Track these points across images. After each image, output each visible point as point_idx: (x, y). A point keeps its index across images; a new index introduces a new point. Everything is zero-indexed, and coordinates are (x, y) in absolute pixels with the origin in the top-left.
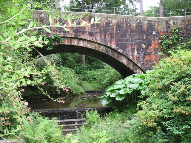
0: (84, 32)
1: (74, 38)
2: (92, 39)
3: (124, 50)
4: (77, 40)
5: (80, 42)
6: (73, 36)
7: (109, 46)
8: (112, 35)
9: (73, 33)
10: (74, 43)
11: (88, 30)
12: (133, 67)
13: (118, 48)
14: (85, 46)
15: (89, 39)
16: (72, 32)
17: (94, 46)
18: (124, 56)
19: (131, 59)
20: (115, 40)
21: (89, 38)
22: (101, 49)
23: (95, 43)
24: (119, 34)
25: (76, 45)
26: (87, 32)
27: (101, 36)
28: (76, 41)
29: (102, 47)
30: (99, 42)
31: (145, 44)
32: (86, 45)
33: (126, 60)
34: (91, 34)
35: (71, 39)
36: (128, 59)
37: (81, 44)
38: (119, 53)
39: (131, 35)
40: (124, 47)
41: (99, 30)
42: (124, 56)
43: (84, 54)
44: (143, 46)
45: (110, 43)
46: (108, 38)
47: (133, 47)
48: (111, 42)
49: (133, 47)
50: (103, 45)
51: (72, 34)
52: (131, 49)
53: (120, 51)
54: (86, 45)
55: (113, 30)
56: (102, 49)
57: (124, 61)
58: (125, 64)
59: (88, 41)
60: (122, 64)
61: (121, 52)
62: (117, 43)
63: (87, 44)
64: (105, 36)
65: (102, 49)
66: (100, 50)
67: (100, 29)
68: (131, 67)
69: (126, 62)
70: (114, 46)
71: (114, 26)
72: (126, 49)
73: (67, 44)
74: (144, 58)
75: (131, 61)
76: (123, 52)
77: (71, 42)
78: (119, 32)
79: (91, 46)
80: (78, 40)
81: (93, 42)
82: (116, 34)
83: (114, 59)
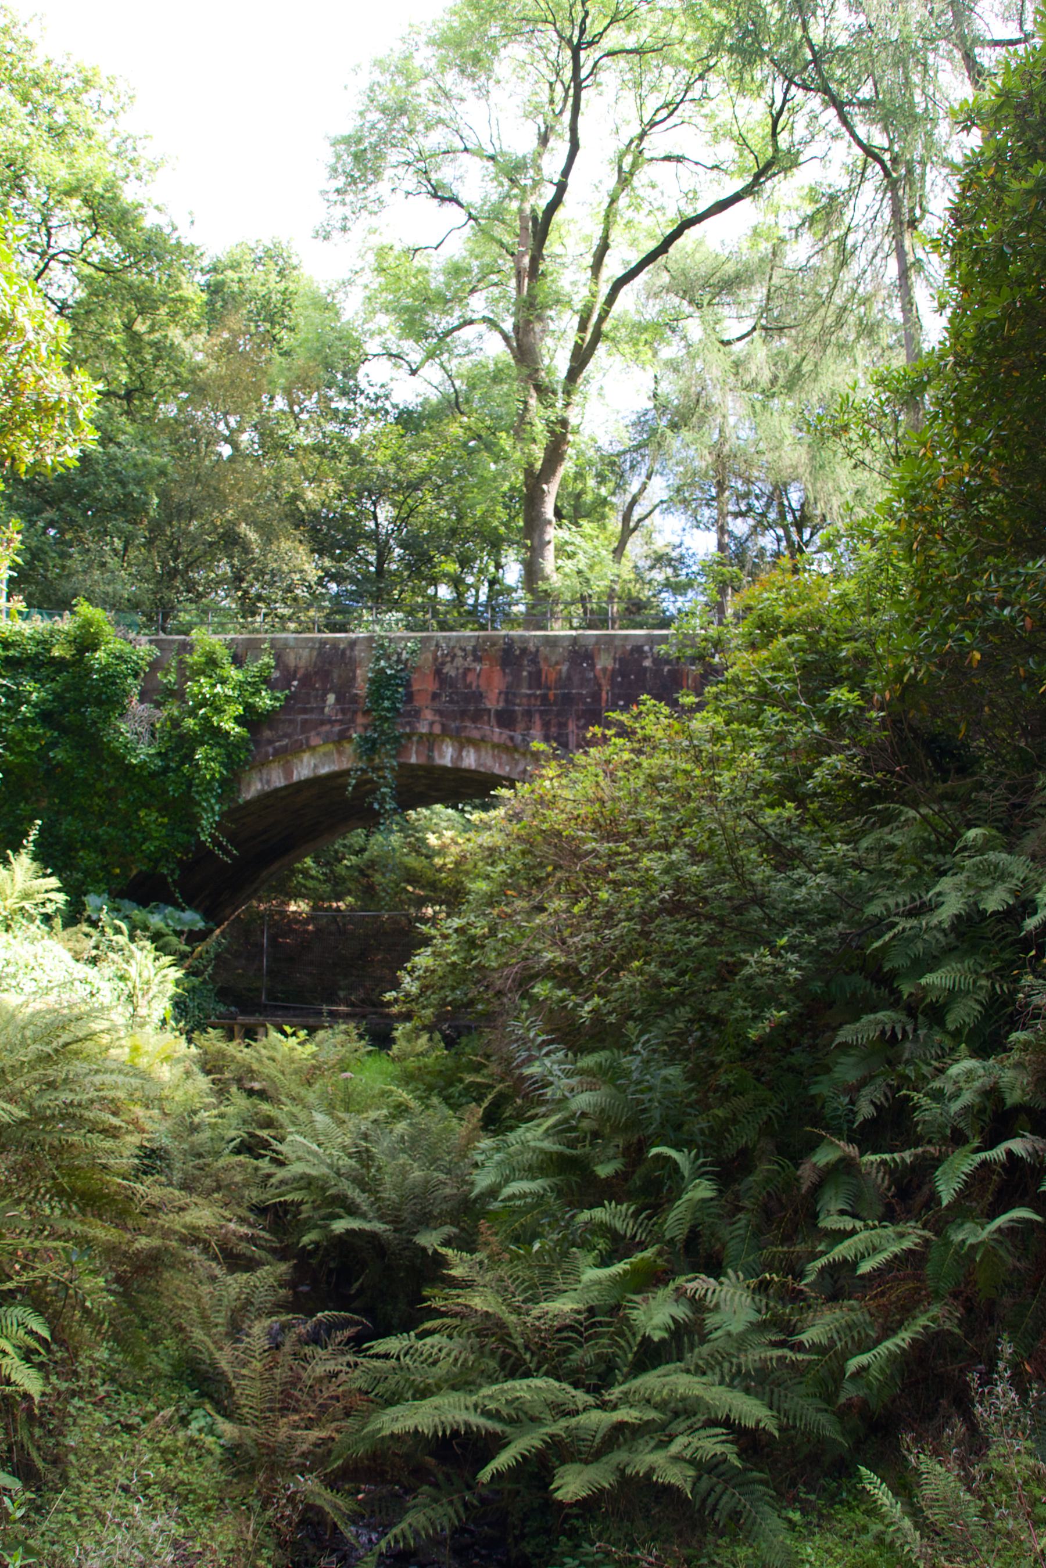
10: (442, 756)
32: (489, 762)
54: (489, 762)
64: (563, 725)
67: (544, 698)
71: (603, 682)
73: (413, 760)
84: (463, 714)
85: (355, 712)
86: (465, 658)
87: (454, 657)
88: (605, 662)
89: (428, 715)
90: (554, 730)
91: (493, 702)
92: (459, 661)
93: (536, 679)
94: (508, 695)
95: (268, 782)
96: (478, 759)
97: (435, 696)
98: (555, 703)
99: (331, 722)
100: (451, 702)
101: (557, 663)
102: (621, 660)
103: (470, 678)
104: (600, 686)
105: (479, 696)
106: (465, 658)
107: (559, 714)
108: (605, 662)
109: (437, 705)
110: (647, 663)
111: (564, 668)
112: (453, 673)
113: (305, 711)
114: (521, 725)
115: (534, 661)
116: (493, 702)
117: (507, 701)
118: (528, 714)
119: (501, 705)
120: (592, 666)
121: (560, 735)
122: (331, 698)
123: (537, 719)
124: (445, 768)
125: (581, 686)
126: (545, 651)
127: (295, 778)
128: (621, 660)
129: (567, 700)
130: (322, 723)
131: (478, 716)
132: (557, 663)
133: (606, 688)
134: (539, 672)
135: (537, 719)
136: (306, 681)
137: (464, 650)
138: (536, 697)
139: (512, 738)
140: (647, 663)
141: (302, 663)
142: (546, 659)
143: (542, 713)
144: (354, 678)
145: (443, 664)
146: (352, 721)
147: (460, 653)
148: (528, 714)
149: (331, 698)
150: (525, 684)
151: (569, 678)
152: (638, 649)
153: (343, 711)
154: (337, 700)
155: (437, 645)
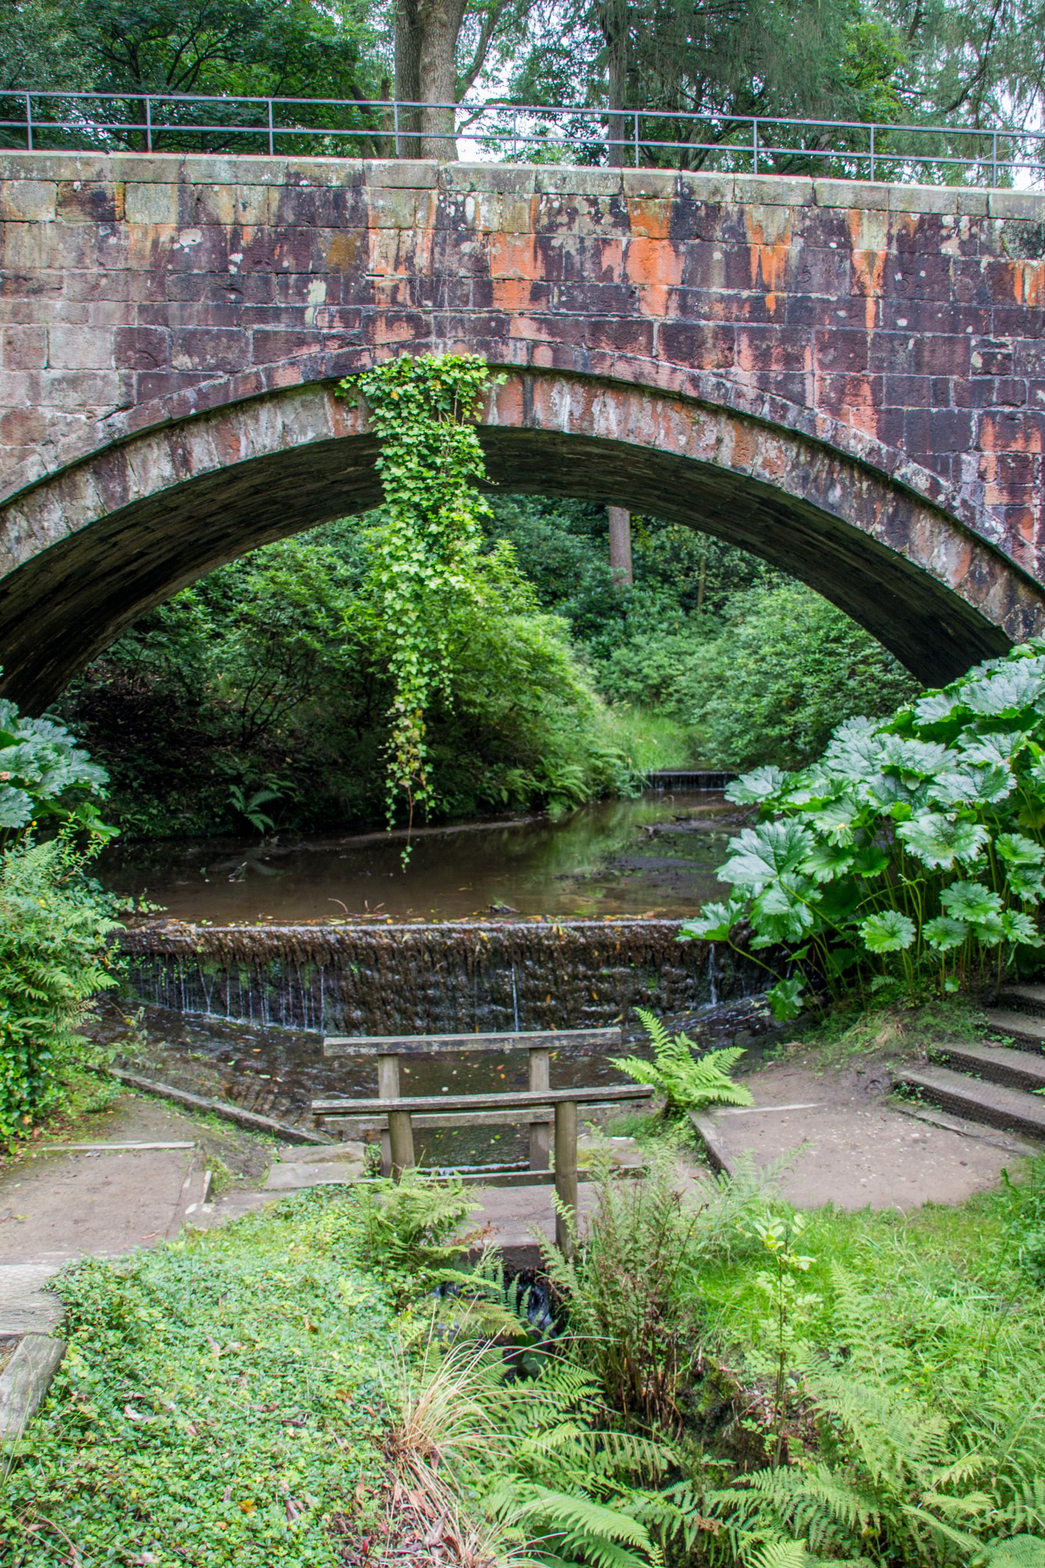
0: (629, 332)
1: (552, 375)
3: (944, 472)
4: (573, 395)
5: (596, 408)
6: (544, 359)
7: (824, 435)
8: (848, 347)
9: (544, 337)
10: (551, 409)
11: (662, 312)
12: (1012, 599)
13: (892, 457)
14: (632, 440)
15: (663, 381)
16: (535, 326)
17: (710, 438)
18: (943, 515)
19: (993, 540)
20: (875, 393)
21: (666, 374)
22: (759, 460)
23: (715, 411)
24: (907, 338)
25: (566, 430)
26: (650, 324)
27: (762, 358)
28: (568, 399)
29: (769, 448)
30: (744, 406)
33: (958, 545)
34: (681, 342)
35: (528, 379)
36: (976, 541)
37: (609, 420)
38: (903, 491)
39: (1003, 345)
40: (941, 444)
41: (747, 308)
42: (943, 515)
43: (626, 505)
45: (836, 411)
46: (815, 377)
47: (1017, 446)
48: (840, 401)
49: (1017, 446)
50: (774, 429)
51: (535, 344)
52: (1001, 460)
53: (916, 476)
55: (855, 305)
56: (767, 464)
57: (942, 559)
58: (951, 581)
60: (926, 583)
62: (889, 412)
63: (654, 415)
64: (792, 360)
65: (769, 462)
66: (754, 466)
67: (757, 305)
68: (992, 602)
69: (952, 567)
70: (860, 435)
72: (958, 462)
75: (994, 554)
76: (935, 488)
77: (527, 405)
78: (903, 322)
79: (683, 440)
80: (580, 390)
81: (699, 404)
82: (890, 339)
83: (862, 546)
84: (597, 329)
85: (371, 320)
86: (597, 218)
87: (573, 214)
88: (871, 240)
89: (524, 329)
90: (777, 370)
91: (656, 309)
92: (583, 224)
93: (739, 268)
94: (685, 297)
95: (185, 462)
96: (623, 421)
97: (537, 293)
98: (778, 318)
99: (323, 340)
100: (570, 304)
101: (781, 238)
102: (901, 239)
103: (610, 258)
104: (862, 287)
105: (627, 296)
106: (597, 218)
107: (786, 338)
108: (871, 240)
109: (541, 307)
110: (950, 248)
111: (794, 247)
112: (571, 247)
113: (262, 315)
114: (711, 357)
115: (737, 233)
116: (656, 309)
117: (683, 308)
118: (726, 335)
119: (673, 316)
120: (847, 246)
121: (788, 378)
122: (318, 291)
123: (743, 343)
124: (556, 435)
125: (827, 287)
126: (757, 214)
127: (244, 452)
128: (901, 239)
129: (800, 313)
130: (301, 342)
131: (629, 332)
132: (781, 238)
133: (874, 290)
134: (748, 250)
135: (743, 343)
136: (260, 255)
137: (593, 203)
138: (741, 302)
139: (695, 381)
140: (950, 248)
141: (249, 217)
142: (759, 229)
143: (755, 335)
144: (366, 250)
145: (552, 227)
146: (366, 336)
147: (584, 208)
148: (726, 335)
149: (318, 291)
150: (718, 277)
151: (804, 270)
152: (932, 222)
153: (346, 318)
154: (330, 294)
155: (538, 189)
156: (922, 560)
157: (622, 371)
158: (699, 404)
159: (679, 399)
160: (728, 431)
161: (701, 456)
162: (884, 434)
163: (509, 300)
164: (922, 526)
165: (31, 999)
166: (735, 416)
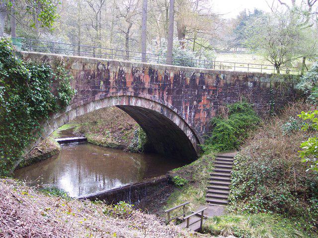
2: (151, 97)
17: (151, 106)
21: (148, 96)
27: (159, 93)
31: (196, 101)
34: (150, 91)
38: (174, 112)
44: (195, 103)
50: (159, 104)
53: (175, 110)
55: (170, 85)
57: (177, 121)
59: (146, 99)
61: (176, 111)
64: (163, 93)
65: (158, 109)
73: (124, 104)
74: (194, 116)
81: (152, 101)
156: (174, 122)
157: (142, 96)
158: (152, 101)
159: (149, 100)
160: (153, 104)
161: (151, 109)
162: (173, 104)
163: (129, 85)
164: (176, 117)
165: (152, 185)
166: (155, 102)
